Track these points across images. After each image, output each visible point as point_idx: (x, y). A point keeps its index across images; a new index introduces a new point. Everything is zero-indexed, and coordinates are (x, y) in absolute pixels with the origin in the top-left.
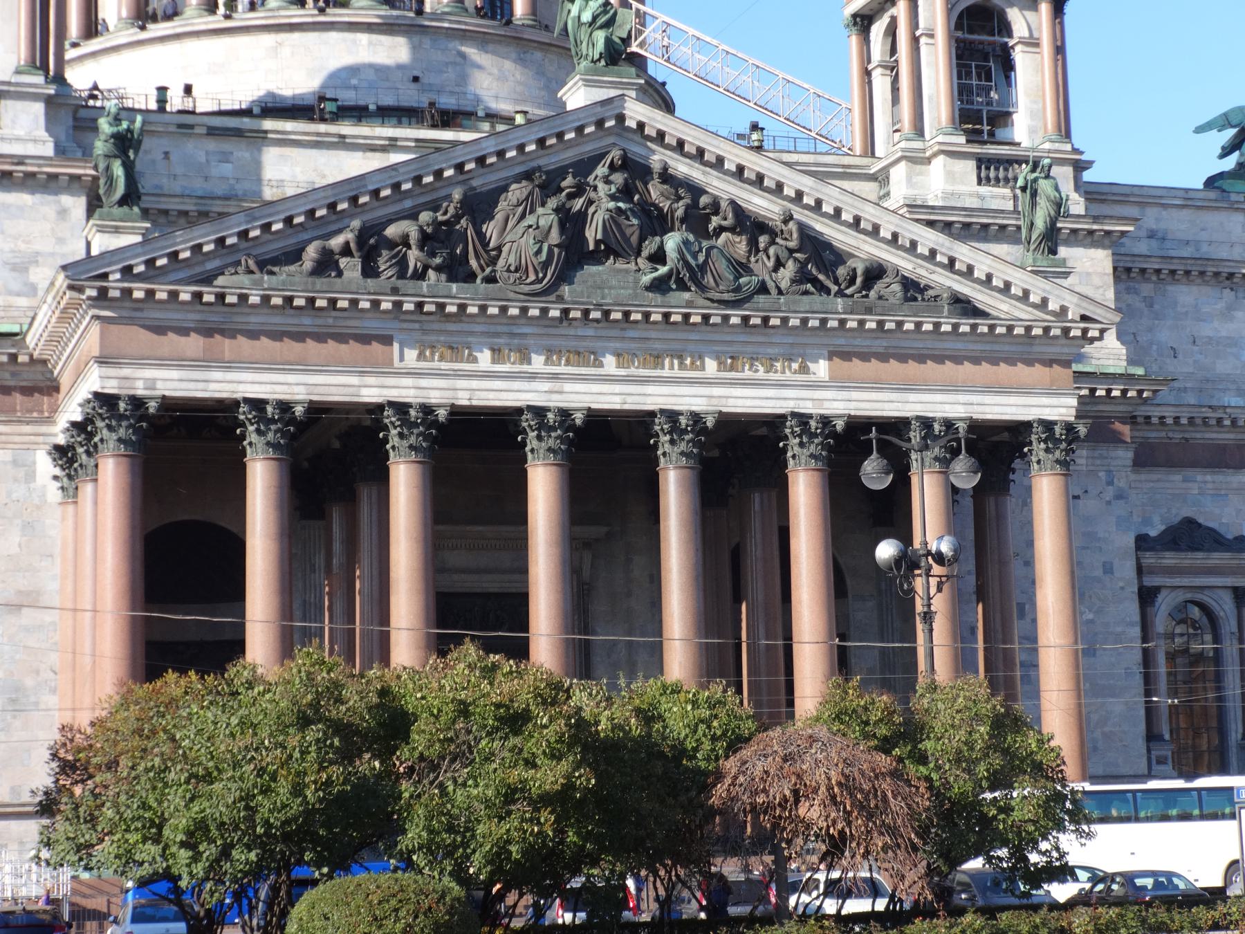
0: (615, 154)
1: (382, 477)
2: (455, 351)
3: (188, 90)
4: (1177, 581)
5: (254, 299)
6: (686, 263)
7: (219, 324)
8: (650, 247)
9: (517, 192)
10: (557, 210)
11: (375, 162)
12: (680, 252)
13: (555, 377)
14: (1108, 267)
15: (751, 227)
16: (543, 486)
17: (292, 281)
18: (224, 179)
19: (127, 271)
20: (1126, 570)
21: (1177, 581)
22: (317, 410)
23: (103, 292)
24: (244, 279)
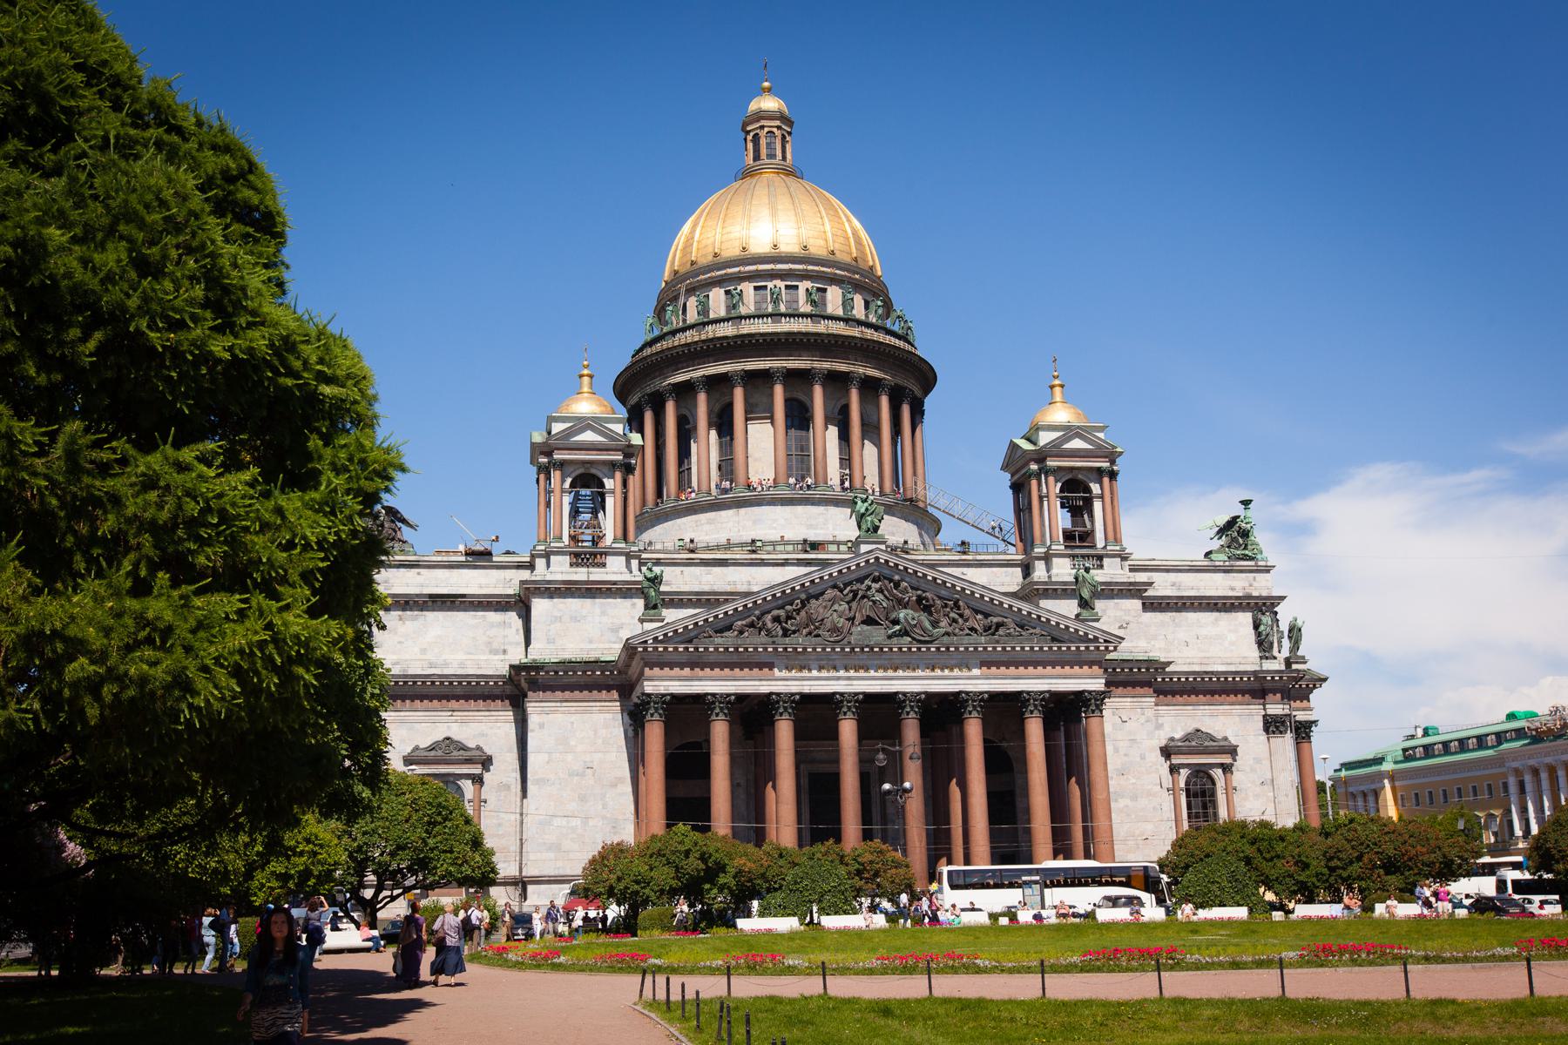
1: (772, 723)
2: (801, 668)
7: (697, 663)
19: (655, 639)
22: (741, 698)
23: (645, 649)
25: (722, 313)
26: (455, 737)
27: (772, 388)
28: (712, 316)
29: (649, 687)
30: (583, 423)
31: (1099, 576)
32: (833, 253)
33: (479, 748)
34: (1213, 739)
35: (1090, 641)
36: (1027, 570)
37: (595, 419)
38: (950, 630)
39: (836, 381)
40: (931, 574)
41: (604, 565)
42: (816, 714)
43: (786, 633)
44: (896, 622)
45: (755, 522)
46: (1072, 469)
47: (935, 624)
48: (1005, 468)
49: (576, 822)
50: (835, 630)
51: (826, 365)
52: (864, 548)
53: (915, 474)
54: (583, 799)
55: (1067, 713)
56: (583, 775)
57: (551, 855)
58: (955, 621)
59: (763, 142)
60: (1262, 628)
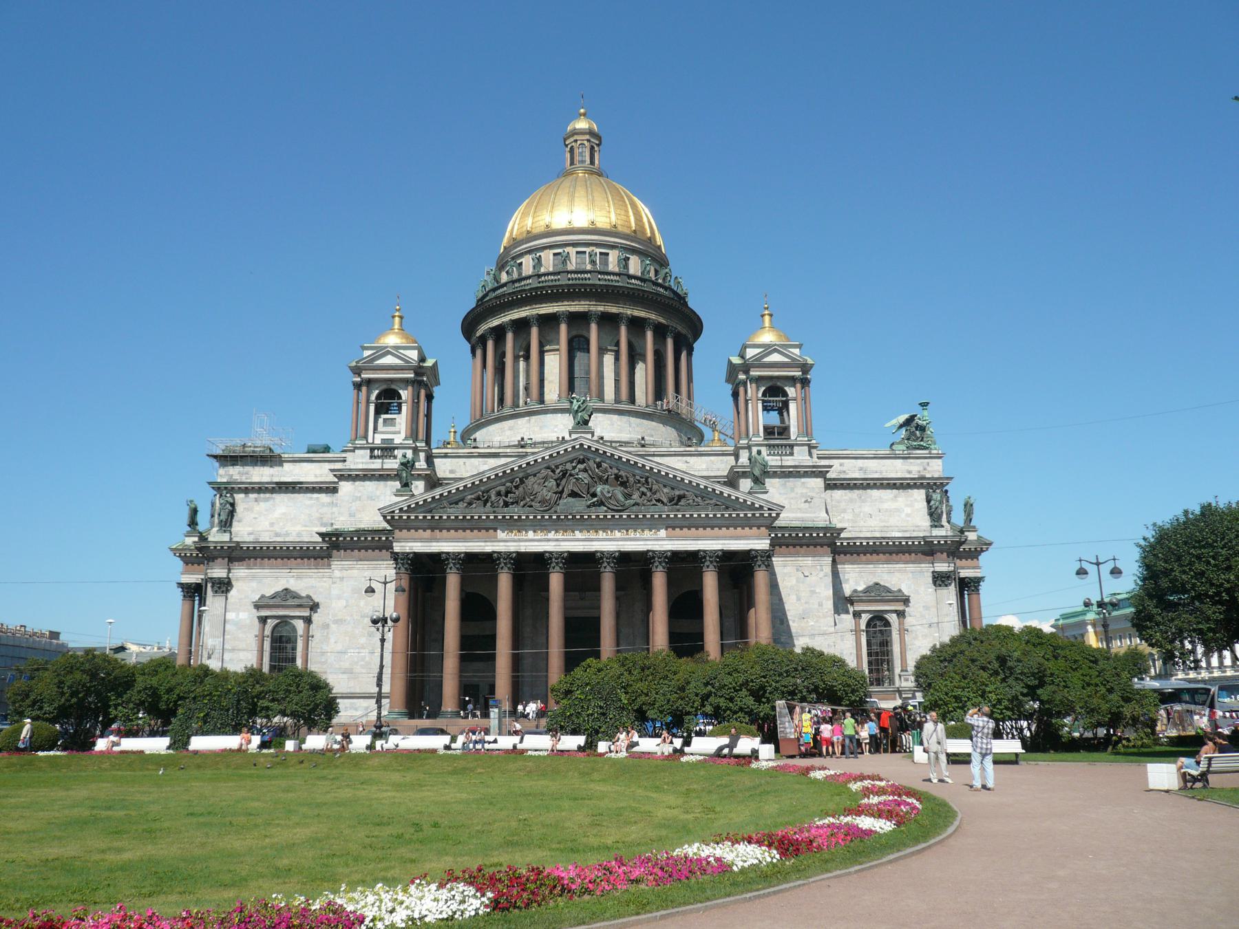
7: (435, 526)
9: (544, 472)
13: (557, 540)
16: (556, 581)
19: (401, 510)
23: (393, 517)
25: (530, 272)
26: (292, 589)
29: (397, 547)
31: (789, 461)
33: (309, 597)
34: (889, 591)
35: (757, 509)
36: (737, 457)
37: (397, 348)
38: (639, 501)
39: (609, 321)
43: (506, 504)
44: (594, 495)
47: (628, 496)
48: (728, 381)
50: (542, 502)
51: (601, 309)
52: (574, 436)
53: (677, 390)
55: (739, 572)
57: (345, 676)
58: (643, 494)
59: (576, 151)
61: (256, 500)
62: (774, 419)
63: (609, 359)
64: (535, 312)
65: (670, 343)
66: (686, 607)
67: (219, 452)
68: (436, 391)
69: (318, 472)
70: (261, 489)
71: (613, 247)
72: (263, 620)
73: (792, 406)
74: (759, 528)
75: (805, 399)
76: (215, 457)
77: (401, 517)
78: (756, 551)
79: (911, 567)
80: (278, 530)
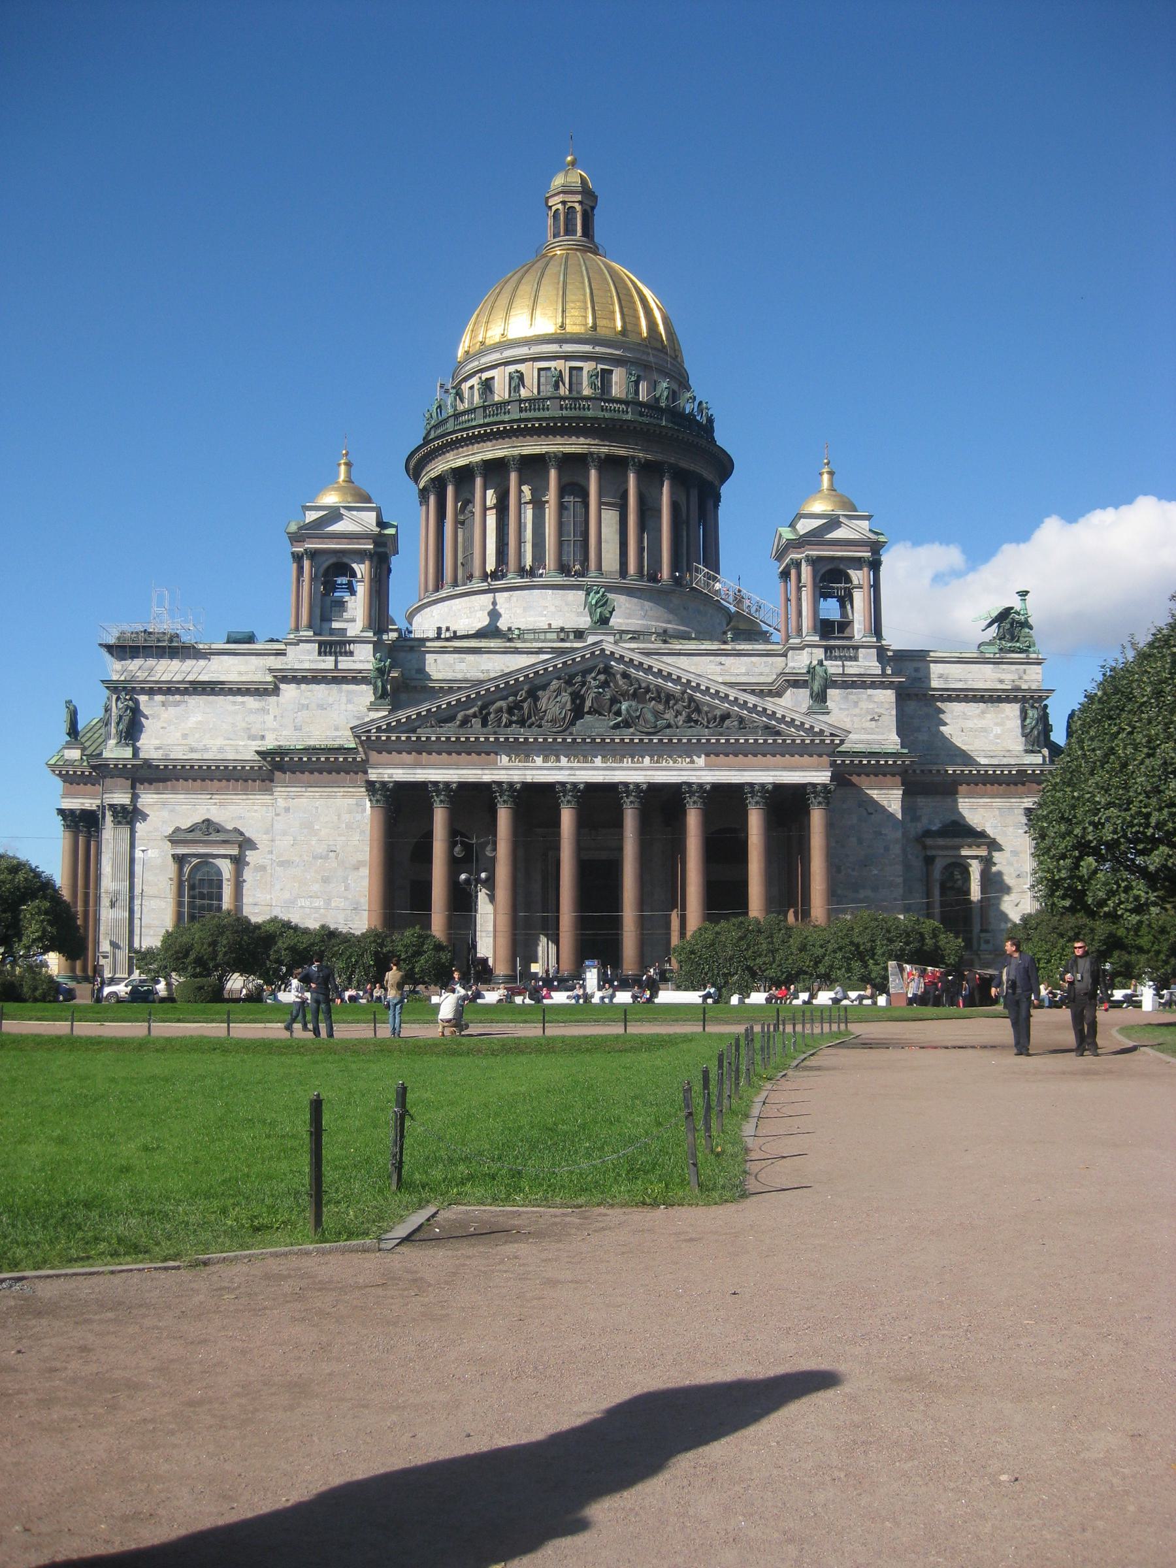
0: (602, 666)
3: (448, 629)
4: (945, 853)
5: (433, 739)
6: (631, 716)
8: (615, 708)
10: (571, 694)
11: (533, 659)
12: (627, 710)
13: (571, 768)
14: (893, 699)
15: (668, 699)
16: (567, 817)
17: (449, 731)
18: (462, 671)
19: (379, 729)
20: (896, 849)
21: (945, 853)
22: (463, 786)
23: (368, 738)
24: (429, 730)
26: (215, 820)
27: (548, 472)
28: (497, 398)
29: (373, 775)
30: (334, 515)
31: (852, 668)
32: (624, 332)
33: (236, 830)
39: (613, 466)
40: (655, 663)
41: (351, 654)
42: (535, 802)
45: (525, 610)
46: (833, 558)
49: (319, 903)
51: (604, 450)
54: (326, 880)
56: (326, 858)
60: (1028, 721)
61: (163, 704)
62: (830, 609)
63: (610, 518)
64: (516, 452)
65: (694, 493)
66: (725, 849)
67: (112, 641)
68: (394, 560)
69: (243, 668)
70: (169, 689)
71: (618, 361)
72: (180, 860)
73: (859, 598)
74: (820, 756)
75: (876, 586)
76: (110, 648)
77: (378, 738)
78: (814, 785)
79: (998, 802)
80: (194, 745)
